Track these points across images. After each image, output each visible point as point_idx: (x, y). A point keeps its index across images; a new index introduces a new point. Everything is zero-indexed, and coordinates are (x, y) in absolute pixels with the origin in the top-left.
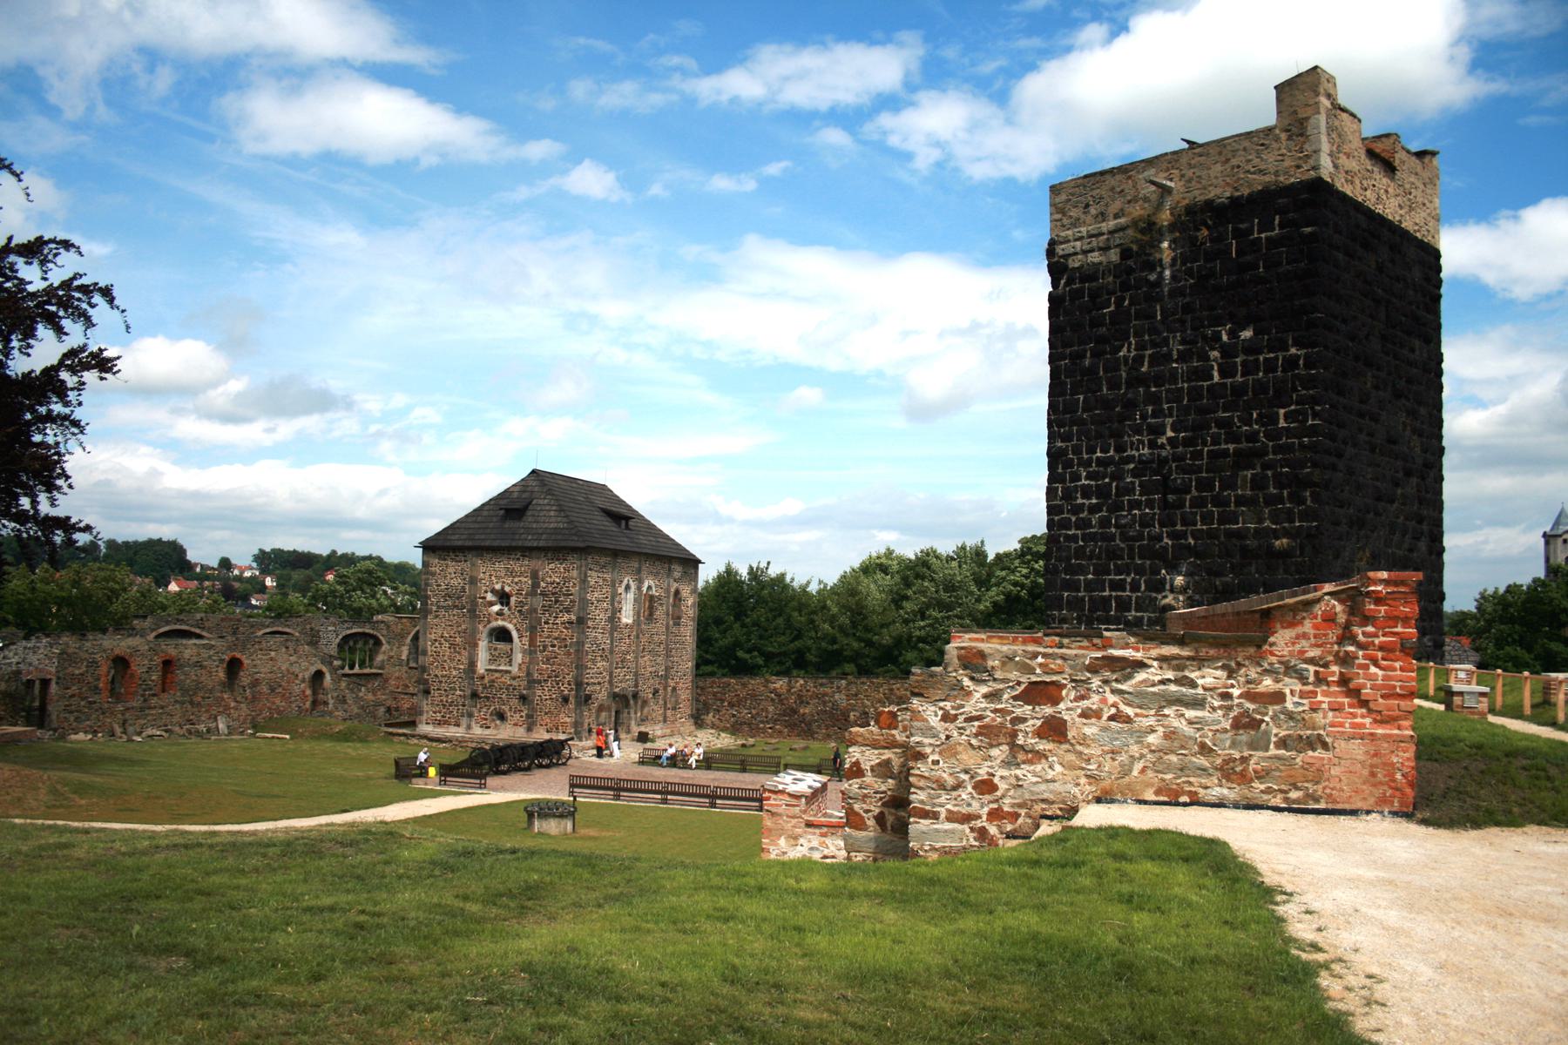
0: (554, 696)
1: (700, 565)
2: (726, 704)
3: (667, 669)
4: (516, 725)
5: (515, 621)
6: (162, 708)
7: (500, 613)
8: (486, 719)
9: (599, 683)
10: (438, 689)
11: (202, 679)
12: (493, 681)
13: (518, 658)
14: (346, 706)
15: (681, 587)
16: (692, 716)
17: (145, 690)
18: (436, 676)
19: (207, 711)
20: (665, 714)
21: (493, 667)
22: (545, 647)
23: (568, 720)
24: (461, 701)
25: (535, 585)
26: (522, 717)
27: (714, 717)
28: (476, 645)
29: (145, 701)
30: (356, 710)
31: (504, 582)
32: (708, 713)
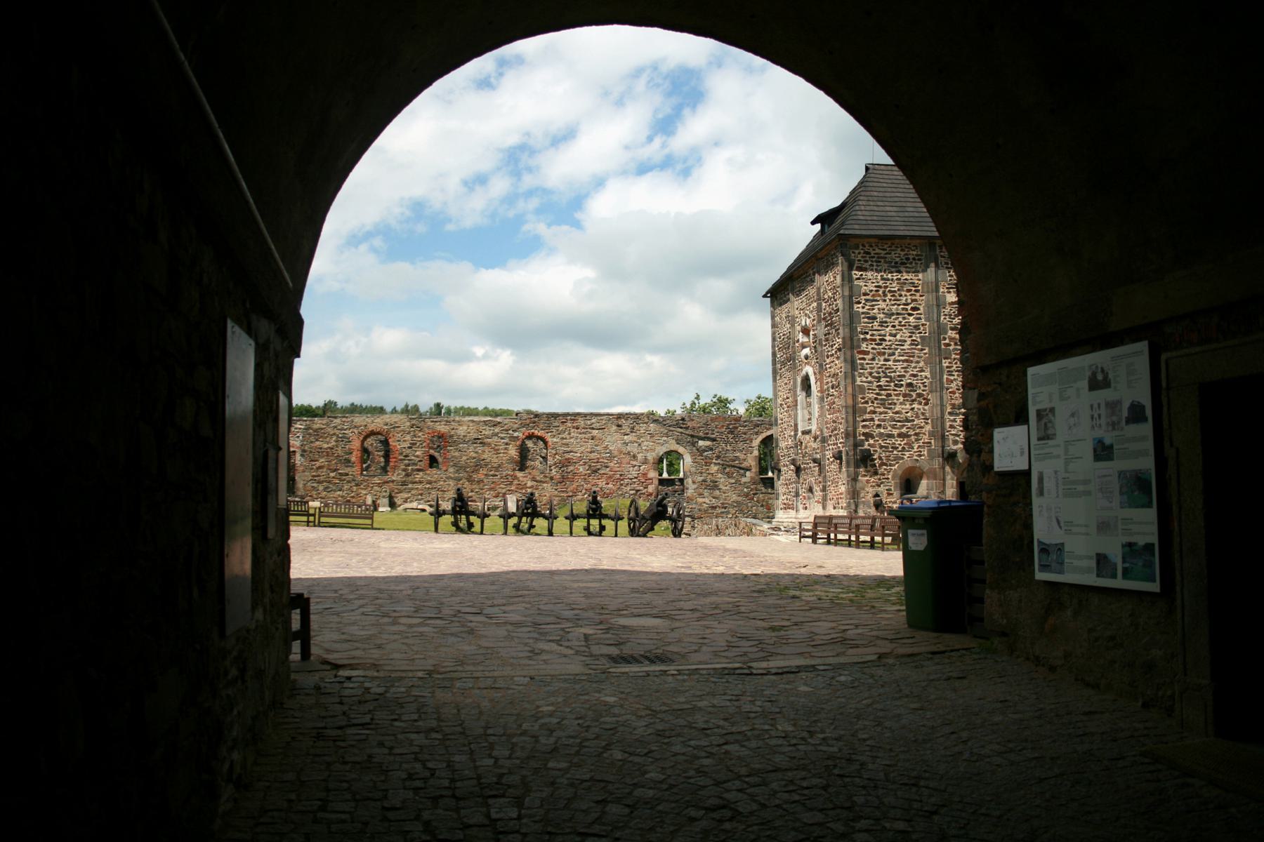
6: (430, 483)
9: (900, 435)
11: (485, 456)
14: (717, 492)
17: (409, 465)
19: (491, 489)
25: (819, 309)
29: (407, 475)
30: (734, 498)
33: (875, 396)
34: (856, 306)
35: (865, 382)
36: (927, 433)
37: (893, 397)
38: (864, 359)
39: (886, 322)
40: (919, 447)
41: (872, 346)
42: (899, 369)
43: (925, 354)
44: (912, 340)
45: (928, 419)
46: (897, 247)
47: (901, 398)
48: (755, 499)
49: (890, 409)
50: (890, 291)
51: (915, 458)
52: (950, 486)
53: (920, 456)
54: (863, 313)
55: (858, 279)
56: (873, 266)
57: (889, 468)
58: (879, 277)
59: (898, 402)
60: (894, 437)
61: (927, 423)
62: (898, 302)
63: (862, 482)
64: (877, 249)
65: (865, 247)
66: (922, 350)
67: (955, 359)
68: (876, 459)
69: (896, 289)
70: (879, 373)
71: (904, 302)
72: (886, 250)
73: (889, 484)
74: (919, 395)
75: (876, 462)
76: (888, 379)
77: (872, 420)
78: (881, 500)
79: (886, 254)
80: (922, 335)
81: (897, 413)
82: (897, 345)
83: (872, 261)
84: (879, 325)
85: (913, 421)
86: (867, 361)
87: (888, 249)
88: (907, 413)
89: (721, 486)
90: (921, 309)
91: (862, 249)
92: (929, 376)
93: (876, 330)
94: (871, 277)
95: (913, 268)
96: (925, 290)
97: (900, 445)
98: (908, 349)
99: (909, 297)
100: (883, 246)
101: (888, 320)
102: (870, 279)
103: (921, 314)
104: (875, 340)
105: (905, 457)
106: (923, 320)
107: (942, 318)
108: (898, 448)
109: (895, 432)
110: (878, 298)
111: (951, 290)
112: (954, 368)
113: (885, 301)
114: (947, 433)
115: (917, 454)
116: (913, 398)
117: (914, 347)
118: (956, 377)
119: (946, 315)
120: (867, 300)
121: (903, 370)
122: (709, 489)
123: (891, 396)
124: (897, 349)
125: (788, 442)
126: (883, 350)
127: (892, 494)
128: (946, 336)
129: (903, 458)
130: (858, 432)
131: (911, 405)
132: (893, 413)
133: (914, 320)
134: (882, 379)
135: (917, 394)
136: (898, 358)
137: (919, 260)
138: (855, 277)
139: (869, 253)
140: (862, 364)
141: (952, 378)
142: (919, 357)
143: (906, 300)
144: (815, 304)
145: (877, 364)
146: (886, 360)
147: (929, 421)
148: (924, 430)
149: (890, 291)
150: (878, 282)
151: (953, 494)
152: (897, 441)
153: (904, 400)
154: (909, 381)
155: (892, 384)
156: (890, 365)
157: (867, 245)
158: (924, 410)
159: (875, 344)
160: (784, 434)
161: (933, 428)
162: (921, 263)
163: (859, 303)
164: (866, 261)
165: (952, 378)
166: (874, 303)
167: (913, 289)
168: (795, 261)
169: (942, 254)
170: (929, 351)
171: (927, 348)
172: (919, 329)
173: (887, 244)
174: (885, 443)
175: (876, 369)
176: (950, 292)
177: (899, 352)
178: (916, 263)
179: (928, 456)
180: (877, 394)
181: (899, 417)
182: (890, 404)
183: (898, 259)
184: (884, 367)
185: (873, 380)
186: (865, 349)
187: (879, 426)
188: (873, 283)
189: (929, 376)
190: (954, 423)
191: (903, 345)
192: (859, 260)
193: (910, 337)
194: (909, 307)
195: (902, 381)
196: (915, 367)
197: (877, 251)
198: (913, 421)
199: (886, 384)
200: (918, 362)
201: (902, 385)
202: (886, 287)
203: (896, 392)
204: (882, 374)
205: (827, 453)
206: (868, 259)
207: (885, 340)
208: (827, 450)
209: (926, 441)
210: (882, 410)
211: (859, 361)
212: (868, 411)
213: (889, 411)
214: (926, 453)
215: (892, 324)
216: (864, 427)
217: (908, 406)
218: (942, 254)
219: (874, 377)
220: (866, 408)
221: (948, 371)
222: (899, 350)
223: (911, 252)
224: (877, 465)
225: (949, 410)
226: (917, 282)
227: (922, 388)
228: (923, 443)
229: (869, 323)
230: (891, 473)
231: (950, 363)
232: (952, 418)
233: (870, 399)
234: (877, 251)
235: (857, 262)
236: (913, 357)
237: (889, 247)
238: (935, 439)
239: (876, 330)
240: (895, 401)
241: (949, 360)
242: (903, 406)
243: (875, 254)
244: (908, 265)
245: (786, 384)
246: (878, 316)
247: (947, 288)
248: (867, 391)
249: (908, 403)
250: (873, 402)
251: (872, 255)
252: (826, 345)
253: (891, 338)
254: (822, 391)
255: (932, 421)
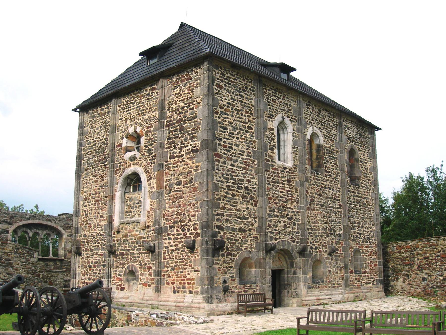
0: (180, 245)
1: (377, 133)
2: (415, 267)
3: (346, 228)
4: (145, 285)
5: (144, 163)
7: (133, 159)
8: (121, 280)
9: (242, 230)
10: (87, 250)
12: (126, 235)
13: (147, 204)
15: (356, 148)
16: (381, 282)
18: (85, 236)
20: (347, 277)
21: (126, 220)
22: (171, 186)
23: (194, 275)
24: (102, 259)
25: (162, 117)
26: (150, 275)
27: (404, 282)
28: (112, 198)
31: (136, 123)
32: (398, 279)
33: (225, 194)
34: (215, 115)
35: (220, 181)
36: (256, 230)
37: (236, 197)
38: (218, 161)
39: (233, 134)
40: (251, 240)
41: (224, 151)
42: (240, 174)
43: (255, 165)
44: (248, 152)
45: (256, 218)
46: (240, 76)
47: (241, 198)
48: (41, 276)
49: (234, 206)
50: (236, 109)
51: (249, 250)
52: (268, 274)
53: (251, 248)
54: (219, 122)
55: (217, 93)
56: (226, 86)
57: (233, 257)
58: (230, 96)
59: (239, 201)
60: (236, 231)
61: (256, 221)
62: (240, 120)
63: (215, 269)
64: (229, 74)
65: (222, 69)
66: (254, 161)
67: (271, 172)
68: (224, 249)
69: (240, 109)
70: (228, 175)
71: (243, 120)
72: (234, 76)
73: (233, 272)
74: (252, 198)
75: (224, 252)
76: (233, 181)
77: (223, 215)
78: (228, 286)
79: (234, 79)
80: (254, 149)
81: (238, 210)
82: (239, 154)
83: (225, 82)
84: (229, 135)
85: (248, 218)
86: (220, 164)
87: (236, 76)
88: (244, 211)
89: (14, 264)
90: (254, 129)
91: (220, 71)
92: (257, 183)
93: (226, 139)
94: (225, 95)
95: (249, 95)
96: (256, 115)
97: (240, 238)
98: (246, 159)
99: (247, 118)
100: (233, 73)
101: (235, 133)
102: (224, 96)
103: (253, 133)
104: (225, 147)
105: (243, 249)
106: (254, 138)
107: (265, 138)
108: (238, 240)
109: (237, 227)
110: (229, 113)
111: (270, 119)
112: (271, 179)
113: (232, 116)
114: (267, 231)
115: (250, 246)
116: (248, 200)
117: (249, 158)
118: (271, 186)
119: (267, 137)
120: (222, 112)
121: (242, 175)
122: (4, 266)
123: (235, 196)
124: (239, 157)
125: (95, 230)
126: (230, 156)
127: (234, 281)
128: (267, 154)
129: (241, 250)
130: (214, 224)
131: (246, 205)
132: (236, 210)
133: (249, 137)
134: (230, 181)
135: (250, 196)
136: (239, 165)
137: (253, 91)
138: (215, 91)
139: (224, 75)
140: (217, 165)
141: (270, 187)
142: (252, 167)
143: (245, 120)
144: (156, 114)
145: (227, 167)
146: (232, 165)
147: (257, 220)
148: (254, 226)
149: (236, 109)
150: (229, 100)
151: (269, 280)
152: (237, 234)
153: (243, 200)
154: (246, 185)
155: (236, 186)
156: (235, 170)
157: (223, 68)
158: (254, 210)
159: (226, 150)
160: (90, 224)
161: (259, 226)
162: (254, 94)
163: (217, 113)
164: (222, 81)
165: (270, 187)
166: (226, 116)
167: (250, 112)
168: (106, 86)
169: (265, 90)
170: (258, 162)
171: (256, 160)
172: (252, 144)
173: (235, 72)
174: (231, 236)
175: (226, 172)
176: (269, 120)
177: (240, 160)
178: (251, 93)
179: (256, 249)
180: (227, 193)
181: (239, 214)
182: (234, 203)
183: (241, 86)
184: (231, 170)
185: (224, 180)
186: (220, 153)
187: (227, 220)
188: (226, 100)
189: (257, 183)
190: (270, 223)
191: (243, 155)
192: (218, 79)
193: (247, 149)
194: (247, 125)
195: (242, 184)
196: (249, 174)
197: (229, 75)
198: (248, 218)
199: (232, 185)
200: (251, 171)
201: (242, 187)
202: (234, 105)
203: (238, 193)
204: (230, 177)
205: (164, 242)
206: (223, 79)
207: (232, 148)
208: (166, 239)
209: (255, 236)
210: (228, 207)
211: (215, 163)
212: (221, 206)
213: (234, 209)
214: (255, 246)
215: (237, 136)
216: (218, 220)
217: (245, 206)
218: (265, 90)
219: (225, 178)
220: (219, 203)
221: (268, 181)
222: (240, 159)
223: (248, 83)
224: (225, 254)
225: (268, 212)
226: (251, 107)
227: (254, 192)
228: (254, 237)
229: (222, 132)
230: (234, 262)
231: (269, 175)
232: (270, 218)
233: (222, 196)
234: (229, 75)
235: (216, 80)
236: (248, 166)
237: (236, 75)
238: (261, 235)
239: (226, 139)
240: (237, 200)
241: (268, 173)
242: (242, 206)
243: (228, 77)
244: (246, 92)
245: (96, 181)
246: (229, 127)
247: (268, 117)
248: (220, 189)
249: (245, 203)
250: (223, 200)
251: (226, 77)
252: (169, 148)
253: (236, 148)
254: (160, 186)
255: (259, 220)
